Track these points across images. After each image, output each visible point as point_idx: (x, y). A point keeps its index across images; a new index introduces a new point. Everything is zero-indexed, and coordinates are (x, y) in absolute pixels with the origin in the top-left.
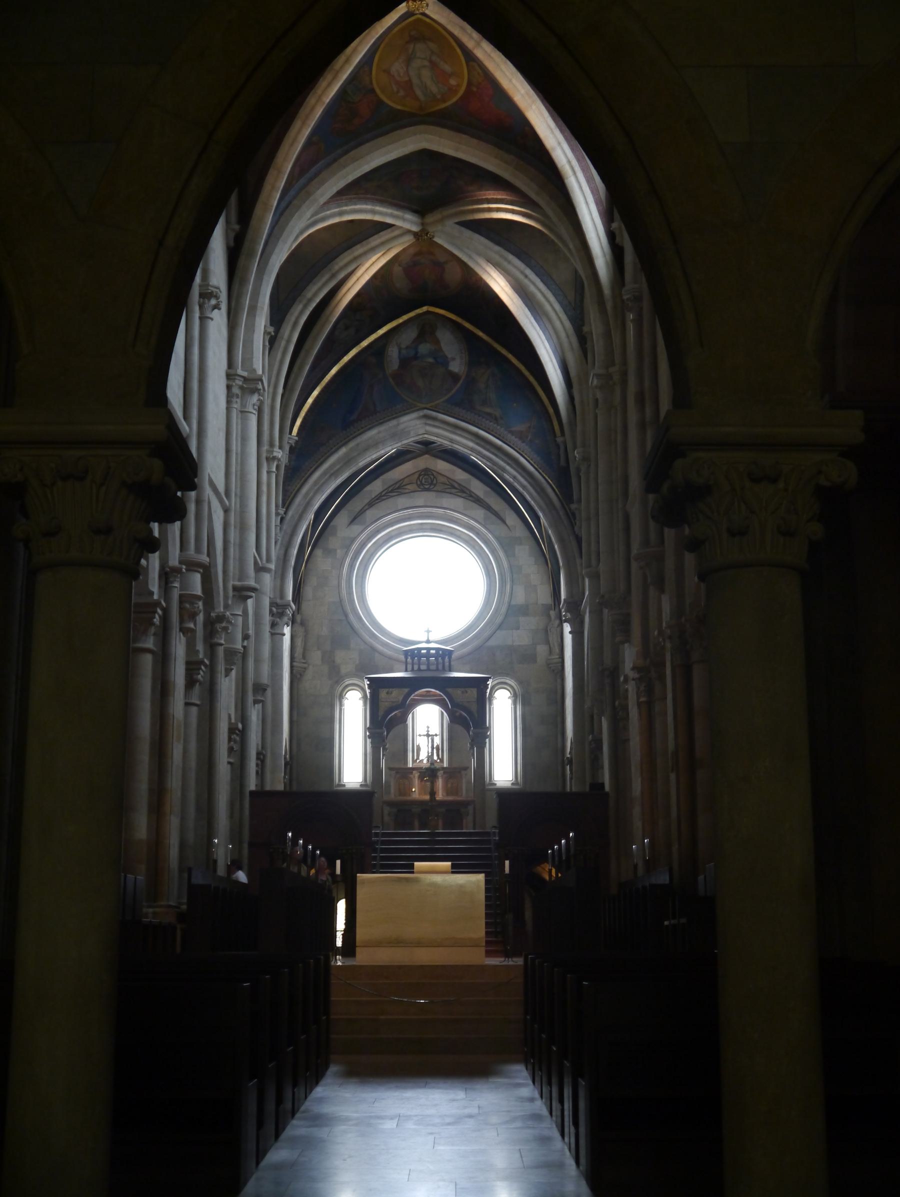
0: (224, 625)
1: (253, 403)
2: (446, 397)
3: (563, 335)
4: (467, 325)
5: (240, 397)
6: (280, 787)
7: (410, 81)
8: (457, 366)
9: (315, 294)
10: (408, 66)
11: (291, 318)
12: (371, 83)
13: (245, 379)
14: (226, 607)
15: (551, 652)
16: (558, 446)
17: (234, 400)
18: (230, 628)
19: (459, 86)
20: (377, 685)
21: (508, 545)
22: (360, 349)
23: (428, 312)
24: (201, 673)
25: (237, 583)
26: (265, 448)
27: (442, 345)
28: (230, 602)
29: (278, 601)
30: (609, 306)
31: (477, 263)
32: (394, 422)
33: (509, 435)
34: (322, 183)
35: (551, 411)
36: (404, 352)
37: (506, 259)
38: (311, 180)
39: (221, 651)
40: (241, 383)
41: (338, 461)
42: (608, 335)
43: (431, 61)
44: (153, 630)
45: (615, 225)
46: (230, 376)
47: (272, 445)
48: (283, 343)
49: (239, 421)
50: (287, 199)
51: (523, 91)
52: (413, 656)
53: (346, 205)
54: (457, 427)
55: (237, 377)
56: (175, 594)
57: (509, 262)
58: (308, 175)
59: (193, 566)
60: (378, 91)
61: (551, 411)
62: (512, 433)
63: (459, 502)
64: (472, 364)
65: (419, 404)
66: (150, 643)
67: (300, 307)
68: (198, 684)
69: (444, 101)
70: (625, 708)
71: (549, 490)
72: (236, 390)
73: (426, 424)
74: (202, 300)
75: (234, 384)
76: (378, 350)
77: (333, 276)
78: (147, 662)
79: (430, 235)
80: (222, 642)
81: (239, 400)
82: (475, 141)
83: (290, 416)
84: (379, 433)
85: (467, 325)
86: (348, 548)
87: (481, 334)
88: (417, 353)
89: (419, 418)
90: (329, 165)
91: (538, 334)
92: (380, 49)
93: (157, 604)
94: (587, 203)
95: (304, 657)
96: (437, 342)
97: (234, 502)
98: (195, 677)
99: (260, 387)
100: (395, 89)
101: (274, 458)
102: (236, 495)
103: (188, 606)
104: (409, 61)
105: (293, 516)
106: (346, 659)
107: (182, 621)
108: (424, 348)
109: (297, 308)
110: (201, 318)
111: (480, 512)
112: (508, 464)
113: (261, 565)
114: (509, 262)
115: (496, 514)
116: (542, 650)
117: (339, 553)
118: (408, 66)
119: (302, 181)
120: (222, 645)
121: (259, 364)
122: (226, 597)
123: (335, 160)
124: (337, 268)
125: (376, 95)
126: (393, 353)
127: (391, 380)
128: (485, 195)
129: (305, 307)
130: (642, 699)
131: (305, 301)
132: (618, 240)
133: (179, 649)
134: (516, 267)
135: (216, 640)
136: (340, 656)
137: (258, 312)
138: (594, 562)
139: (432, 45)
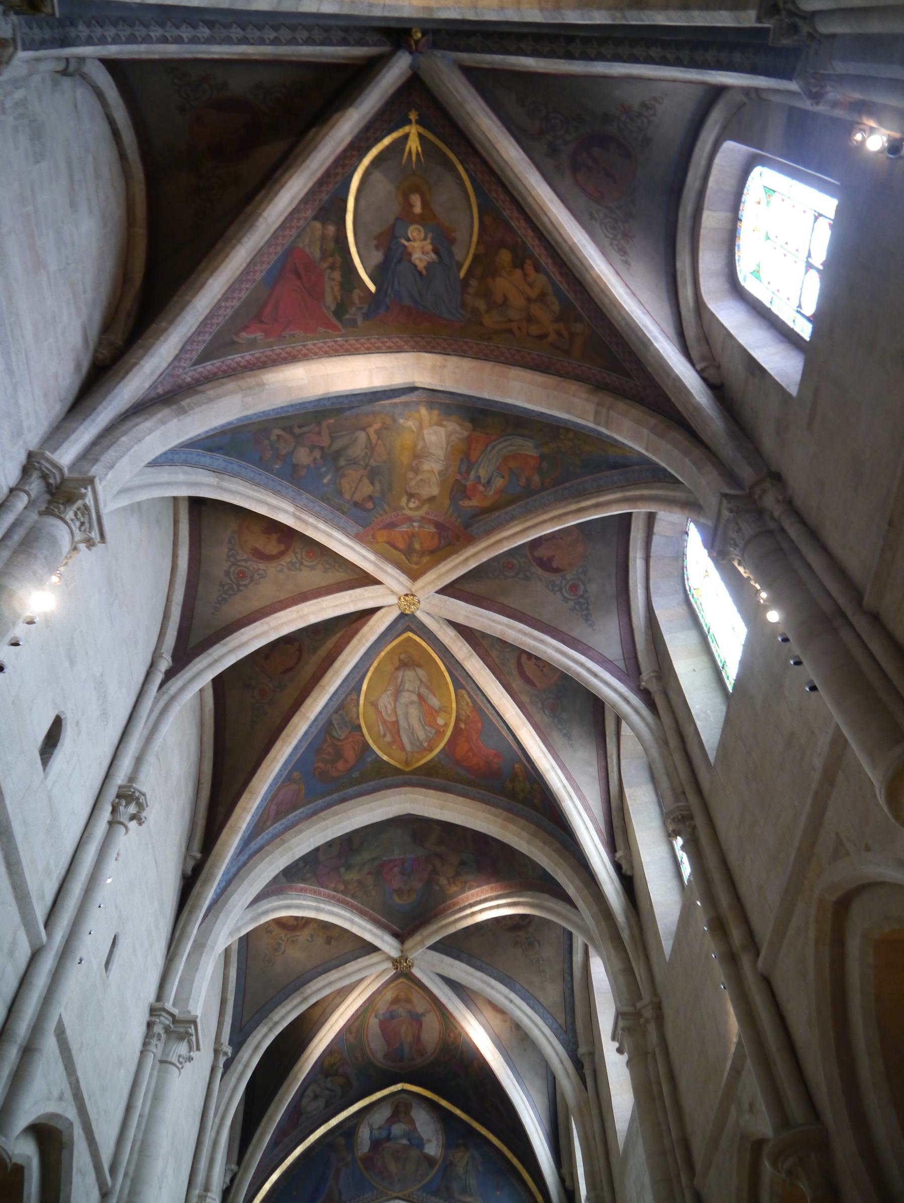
1: (179, 1053)
4: (444, 1103)
7: (396, 723)
8: (433, 1148)
9: (283, 1018)
10: (396, 700)
11: (253, 1041)
12: (358, 718)
13: (175, 1020)
17: (154, 1041)
19: (446, 725)
22: (329, 1128)
23: (403, 1091)
27: (417, 1125)
31: (457, 1008)
34: (300, 832)
36: (376, 1133)
37: (489, 985)
38: (288, 828)
40: (167, 1022)
43: (420, 696)
45: (619, 854)
46: (153, 1011)
48: (240, 1068)
49: (155, 1073)
50: (259, 841)
51: (514, 713)
53: (324, 903)
55: (163, 1014)
57: (492, 988)
58: (285, 821)
60: (365, 730)
64: (448, 1146)
65: (390, 1193)
69: (431, 750)
72: (158, 1029)
74: (117, 800)
75: (158, 1020)
76: (347, 1130)
77: (305, 999)
79: (409, 961)
81: (161, 1045)
82: (461, 799)
85: (444, 1103)
87: (458, 1112)
90: (309, 816)
91: (521, 1098)
92: (369, 675)
94: (587, 828)
96: (412, 1122)
99: (192, 1030)
100: (382, 733)
108: (398, 1129)
109: (262, 1030)
110: (111, 823)
114: (492, 988)
118: (396, 700)
119: (278, 826)
123: (315, 813)
125: (363, 736)
126: (364, 1134)
127: (359, 1163)
128: (468, 898)
129: (271, 1030)
131: (270, 1024)
134: (500, 992)
139: (421, 672)
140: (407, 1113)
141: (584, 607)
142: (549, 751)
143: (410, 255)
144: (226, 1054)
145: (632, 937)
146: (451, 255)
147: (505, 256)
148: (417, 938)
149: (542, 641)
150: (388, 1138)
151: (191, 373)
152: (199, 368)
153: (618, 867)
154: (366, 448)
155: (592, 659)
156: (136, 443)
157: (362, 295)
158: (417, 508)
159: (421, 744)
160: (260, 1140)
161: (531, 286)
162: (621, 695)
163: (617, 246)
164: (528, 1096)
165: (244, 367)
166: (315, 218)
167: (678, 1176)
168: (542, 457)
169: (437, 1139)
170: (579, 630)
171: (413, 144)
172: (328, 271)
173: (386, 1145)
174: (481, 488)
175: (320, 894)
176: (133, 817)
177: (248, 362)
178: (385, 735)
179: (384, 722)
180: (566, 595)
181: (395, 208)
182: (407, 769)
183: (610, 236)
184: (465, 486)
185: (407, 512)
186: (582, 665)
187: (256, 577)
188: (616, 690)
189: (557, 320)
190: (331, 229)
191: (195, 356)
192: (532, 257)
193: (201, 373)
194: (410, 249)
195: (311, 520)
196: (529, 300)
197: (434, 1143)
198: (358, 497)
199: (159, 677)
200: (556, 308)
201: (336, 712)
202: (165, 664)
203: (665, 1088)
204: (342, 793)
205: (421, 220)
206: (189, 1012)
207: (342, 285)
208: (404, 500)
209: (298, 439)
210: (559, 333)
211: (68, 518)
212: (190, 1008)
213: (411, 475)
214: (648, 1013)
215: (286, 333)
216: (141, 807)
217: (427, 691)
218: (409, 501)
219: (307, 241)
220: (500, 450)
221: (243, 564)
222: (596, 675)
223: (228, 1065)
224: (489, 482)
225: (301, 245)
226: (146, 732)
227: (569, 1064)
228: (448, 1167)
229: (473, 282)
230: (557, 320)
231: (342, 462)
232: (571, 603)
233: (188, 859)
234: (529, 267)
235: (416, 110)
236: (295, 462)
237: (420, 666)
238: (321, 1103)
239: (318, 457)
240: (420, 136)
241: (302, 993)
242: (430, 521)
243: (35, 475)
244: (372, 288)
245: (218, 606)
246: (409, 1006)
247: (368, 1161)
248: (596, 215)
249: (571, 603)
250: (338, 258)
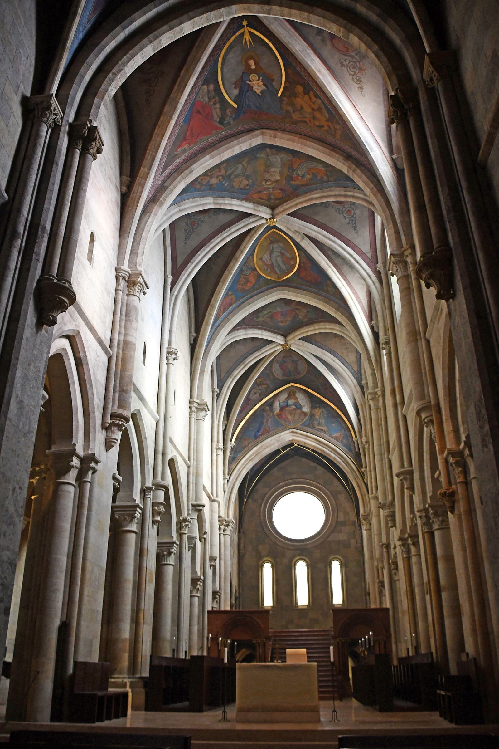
0: (187, 523)
2: (301, 423)
3: (353, 386)
5: (196, 411)
6: (228, 609)
7: (272, 264)
8: (306, 409)
11: (226, 385)
12: (254, 265)
13: (199, 404)
14: (188, 514)
15: (357, 542)
16: (354, 442)
17: (193, 413)
18: (190, 525)
23: (292, 386)
24: (174, 547)
25: (194, 503)
26: (215, 443)
28: (190, 512)
29: (226, 519)
30: (373, 360)
32: (278, 435)
33: (331, 439)
35: (350, 427)
37: (324, 354)
38: (229, 314)
39: (185, 538)
40: (196, 406)
41: (253, 454)
42: (374, 374)
43: (281, 253)
44: (136, 521)
45: (373, 322)
46: (190, 403)
47: (218, 442)
48: (223, 396)
49: (196, 424)
50: (218, 322)
54: (307, 436)
56: (149, 502)
57: (326, 355)
59: (159, 487)
61: (350, 427)
62: (332, 437)
64: (312, 408)
66: (134, 527)
67: (231, 380)
68: (173, 554)
70: (396, 563)
72: (194, 409)
76: (270, 403)
77: (246, 365)
78: (132, 538)
80: (186, 532)
81: (196, 414)
83: (231, 433)
84: (272, 440)
86: (263, 498)
89: (290, 433)
93: (138, 506)
95: (244, 548)
96: (297, 399)
97: (192, 463)
98: (171, 550)
99: (206, 407)
100: (266, 269)
101: (219, 448)
102: (194, 459)
103: (156, 508)
104: (271, 253)
105: (233, 479)
107: (153, 517)
108: (291, 402)
109: (230, 380)
112: (332, 452)
113: (213, 499)
114: (326, 355)
117: (259, 500)
119: (225, 314)
120: (186, 534)
121: (207, 398)
122: (188, 510)
123: (240, 305)
124: (247, 362)
126: (277, 405)
127: (276, 416)
129: (233, 380)
130: (405, 556)
132: (375, 329)
133: (152, 532)
134: (329, 357)
135: (182, 532)
137: (205, 373)
138: (374, 492)
139: (281, 244)
140: (294, 395)
141: (354, 222)
142: (342, 277)
143: (252, 87)
144: (217, 392)
145: (376, 360)
146: (273, 86)
147: (299, 89)
148: (291, 336)
149: (334, 242)
151: (160, 179)
152: (164, 175)
153: (372, 328)
154: (243, 169)
155: (356, 252)
156: (148, 234)
157: (231, 110)
158: (270, 184)
159: (284, 271)
160: (235, 412)
161: (314, 103)
162: (368, 274)
163: (356, 78)
164: (345, 389)
165: (182, 162)
166: (203, 84)
167: (384, 453)
168: (327, 171)
169: (308, 405)
170: (351, 236)
171: (247, 37)
172: (213, 105)
173: (286, 408)
174: (300, 178)
175: (247, 328)
176: (174, 359)
177: (184, 160)
178: (267, 270)
179: (267, 265)
180: (345, 215)
181: (242, 68)
182: (279, 281)
183: (352, 73)
184: (292, 177)
185: (265, 186)
186: (351, 256)
187: (200, 222)
188: (366, 271)
189: (327, 121)
190: (212, 87)
191: (161, 171)
192: (312, 90)
193: (164, 176)
194: (252, 85)
195: (221, 201)
196: (313, 109)
197: (306, 407)
198: (242, 186)
199: (169, 287)
200: (327, 115)
201: (244, 265)
202: (170, 279)
203: (383, 423)
204: (251, 294)
205: (254, 71)
206: (203, 400)
207: (221, 109)
208: (264, 183)
209: (211, 177)
210: (328, 126)
211: (137, 294)
212: (203, 398)
213: (266, 173)
214: (379, 393)
215: (198, 140)
216: (176, 355)
217: (284, 252)
218: (266, 183)
219: (201, 96)
220: (307, 165)
221: (193, 217)
222: (357, 262)
223: (218, 396)
224: (303, 176)
225: (198, 99)
226: (170, 317)
227: (358, 388)
228: (312, 416)
229: (285, 99)
230: (327, 121)
231: (232, 177)
232: (348, 220)
233: (191, 337)
234: (311, 94)
235: (246, 20)
236: (210, 184)
237: (280, 242)
238: (258, 395)
239: (221, 179)
240: (250, 33)
241: (244, 363)
242: (277, 188)
243: (121, 278)
244: (235, 106)
245: (186, 241)
246: (291, 358)
247: (279, 415)
248: (345, 63)
249: (348, 220)
250: (217, 99)
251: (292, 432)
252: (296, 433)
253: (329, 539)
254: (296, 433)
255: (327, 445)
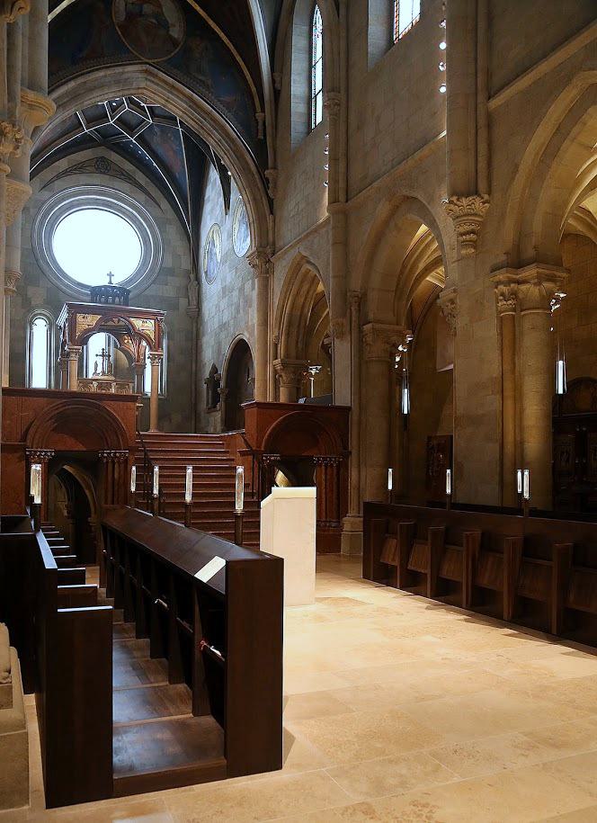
8: (176, 32)
20: (75, 310)
21: (162, 224)
32: (120, 69)
35: (254, 89)
36: (130, 6)
41: (66, 94)
52: (96, 292)
54: (173, 87)
61: (254, 89)
63: (126, 186)
71: (248, 158)
73: (146, 79)
84: (105, 76)
86: (40, 209)
88: (141, 11)
89: (141, 72)
106: (37, 294)
111: (143, 197)
115: (153, 199)
116: (183, 302)
136: (31, 291)
150: (141, 15)
197: (177, 25)
251: (146, 71)
252: (155, 76)
253: (146, 293)
254: (155, 76)
255: (208, 114)
